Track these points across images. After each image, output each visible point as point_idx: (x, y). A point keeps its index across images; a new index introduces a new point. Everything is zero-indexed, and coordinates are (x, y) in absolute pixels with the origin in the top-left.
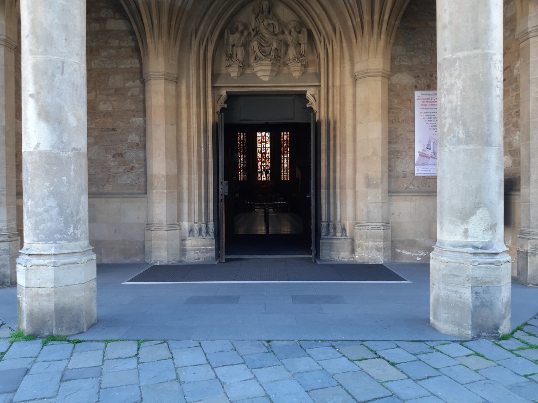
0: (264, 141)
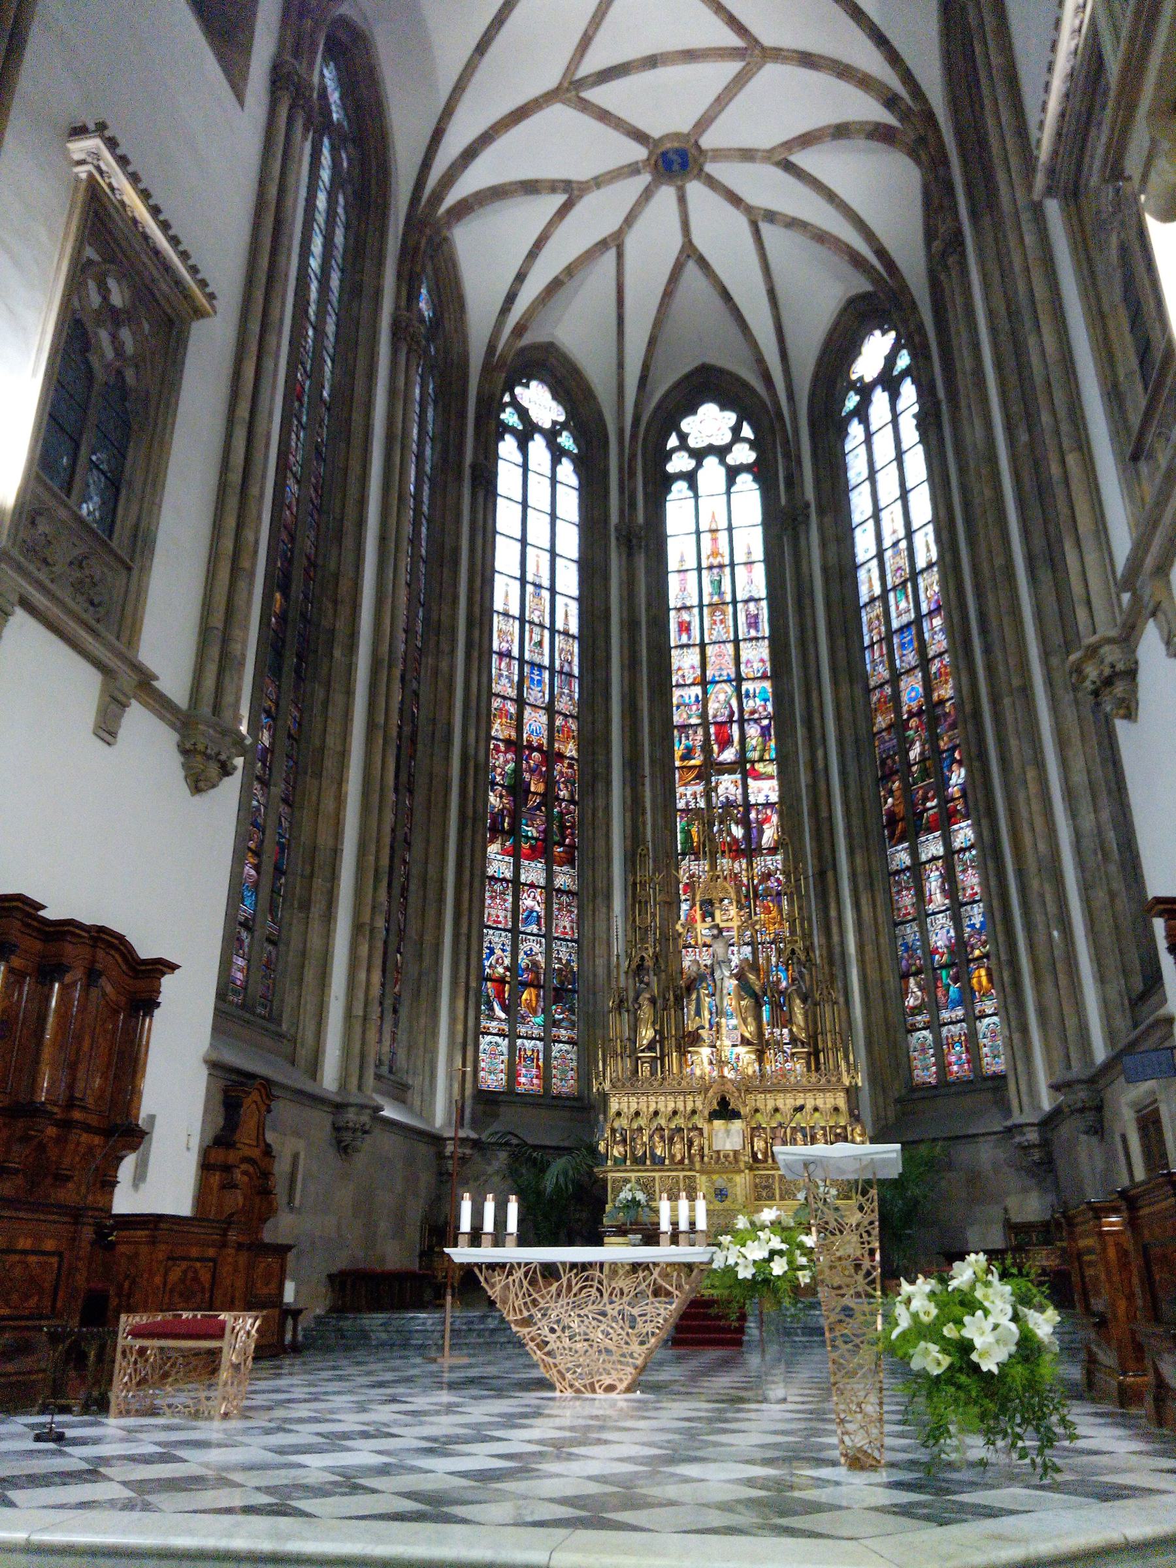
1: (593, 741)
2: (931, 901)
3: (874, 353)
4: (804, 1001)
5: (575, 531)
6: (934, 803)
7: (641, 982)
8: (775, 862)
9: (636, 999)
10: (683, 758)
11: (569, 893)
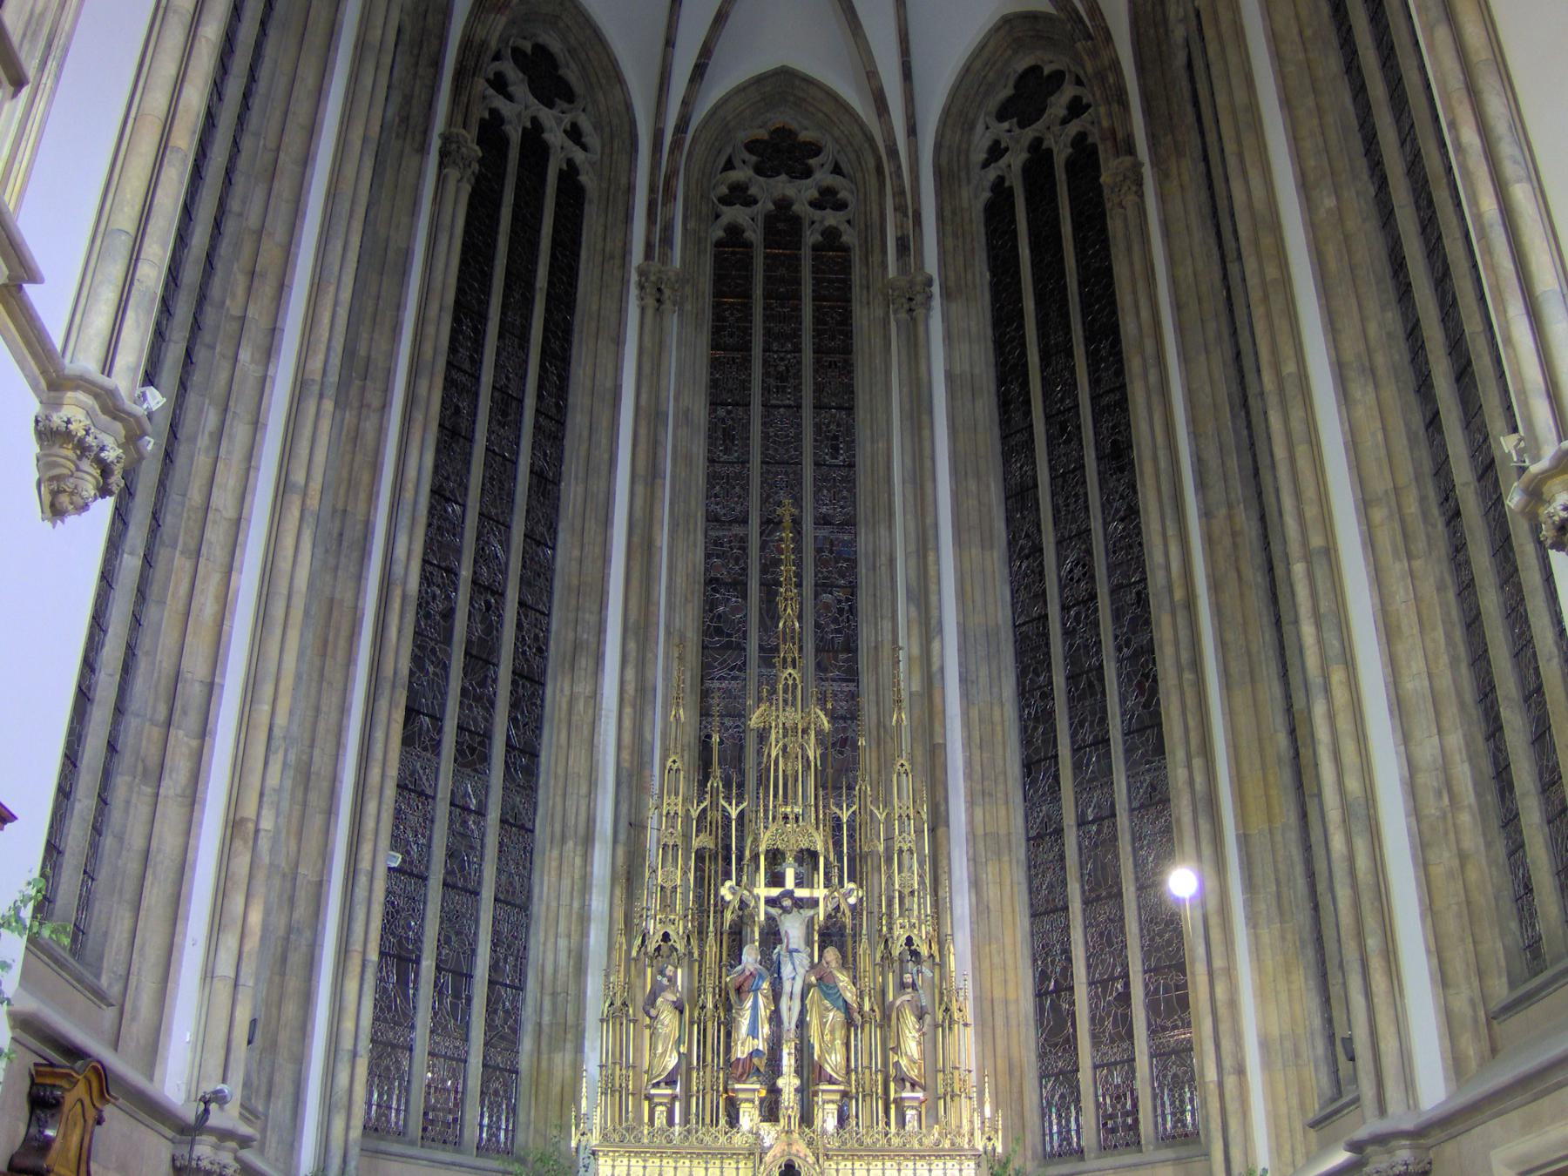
4: (920, 1018)
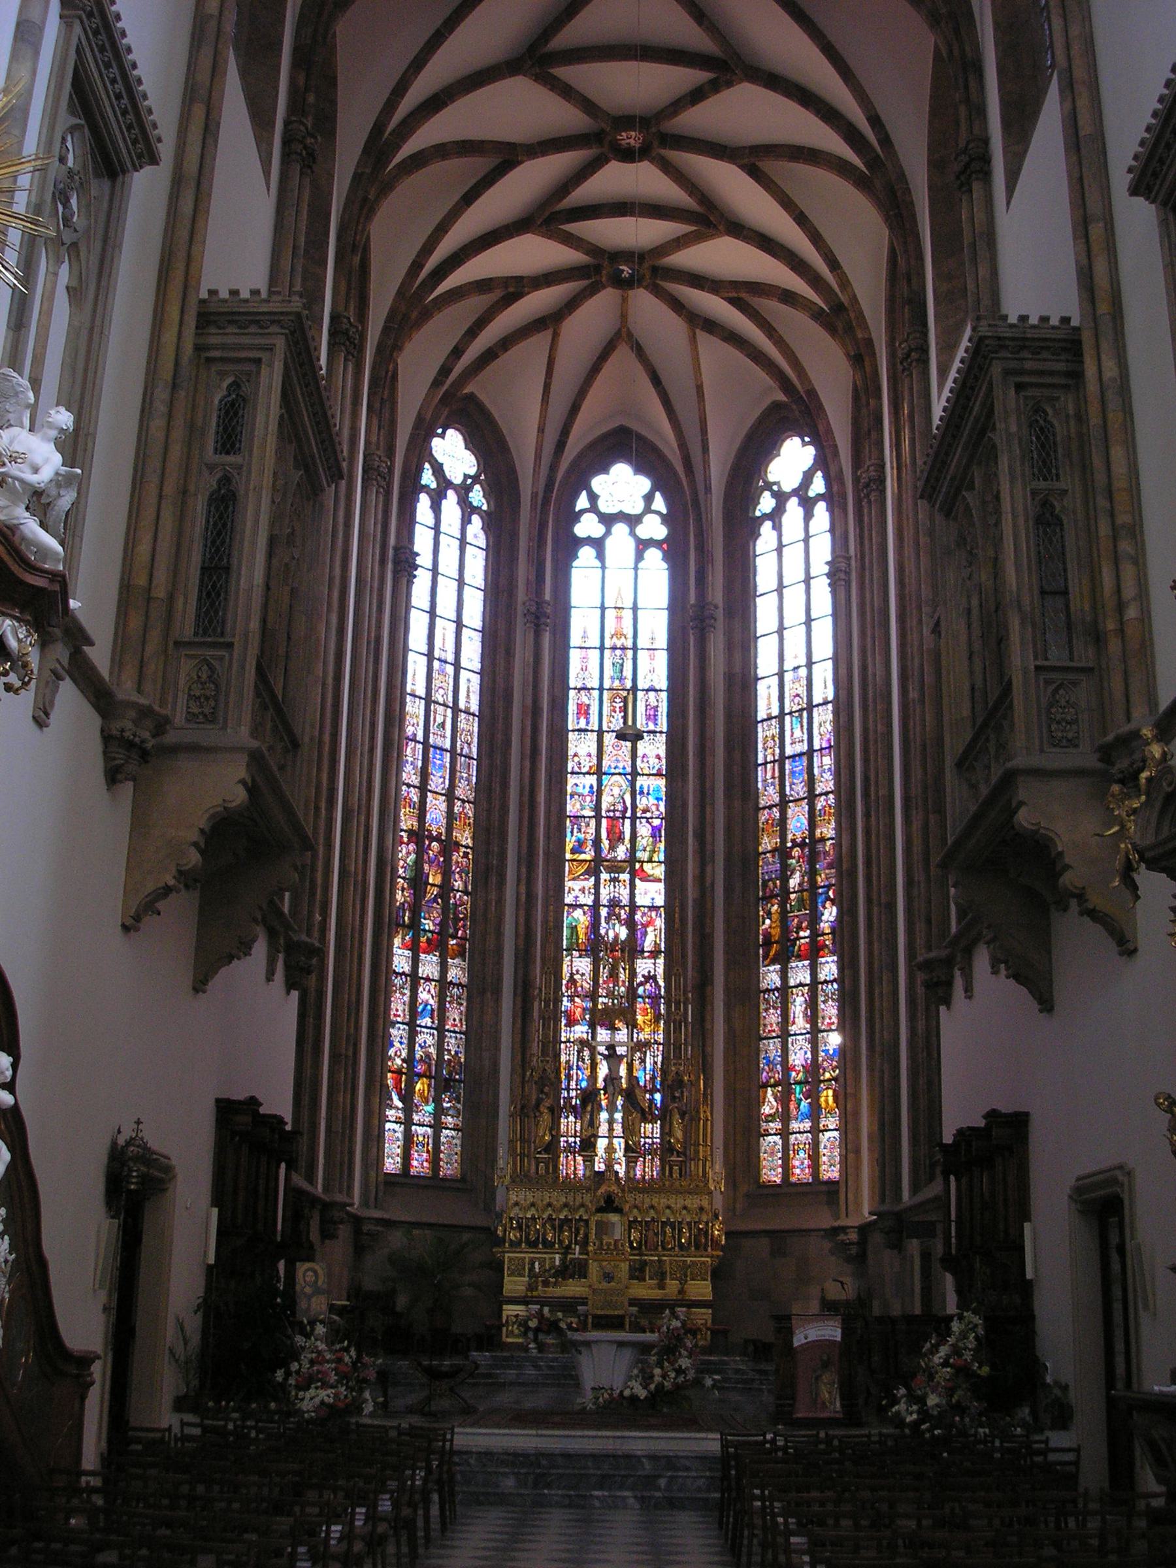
0: (621, 852)
1: (488, 830)
2: (794, 1023)
3: (792, 461)
5: (480, 595)
6: (807, 933)
7: (542, 1092)
8: (659, 967)
9: (537, 1106)
10: (573, 851)
11: (459, 985)
